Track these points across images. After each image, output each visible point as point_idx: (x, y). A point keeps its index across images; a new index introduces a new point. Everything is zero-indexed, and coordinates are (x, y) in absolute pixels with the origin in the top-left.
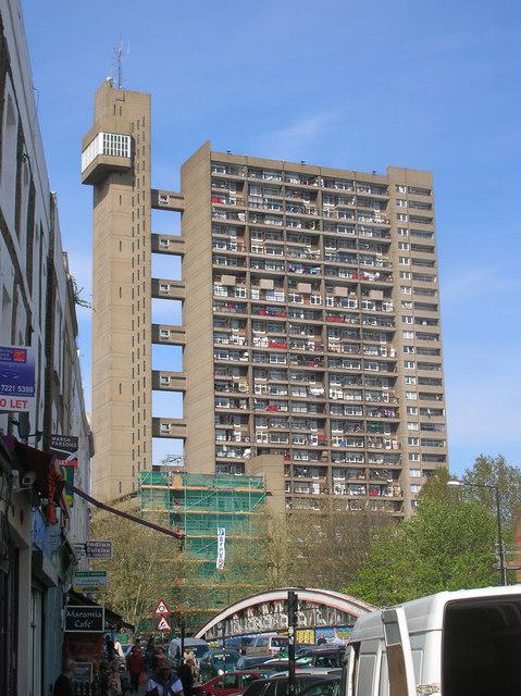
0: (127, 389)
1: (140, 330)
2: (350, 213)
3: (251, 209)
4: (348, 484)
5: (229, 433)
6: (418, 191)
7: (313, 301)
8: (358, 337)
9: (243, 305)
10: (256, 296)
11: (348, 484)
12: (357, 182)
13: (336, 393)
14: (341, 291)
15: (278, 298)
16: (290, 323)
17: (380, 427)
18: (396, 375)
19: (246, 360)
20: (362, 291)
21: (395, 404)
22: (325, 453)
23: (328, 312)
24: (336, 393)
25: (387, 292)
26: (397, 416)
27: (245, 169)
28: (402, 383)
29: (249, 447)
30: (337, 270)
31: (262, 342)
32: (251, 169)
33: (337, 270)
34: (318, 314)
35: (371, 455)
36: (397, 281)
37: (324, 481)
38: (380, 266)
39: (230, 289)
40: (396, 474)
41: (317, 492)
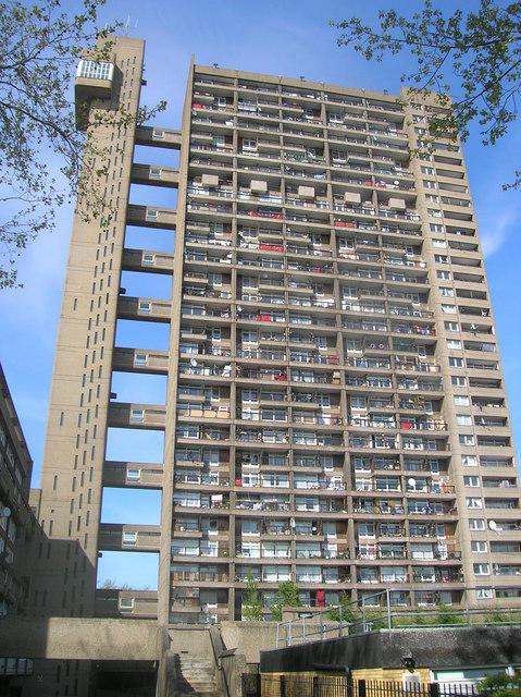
0: (84, 305)
1: (108, 243)
2: (361, 126)
4: (371, 415)
5: (205, 347)
7: (318, 206)
8: (377, 244)
9: (228, 206)
10: (245, 198)
11: (371, 415)
12: (366, 99)
13: (352, 305)
14: (355, 198)
15: (276, 200)
16: (288, 226)
17: (410, 345)
18: (429, 286)
19: (229, 262)
20: (379, 202)
21: (428, 320)
22: (336, 374)
23: (336, 216)
24: (352, 305)
25: (411, 202)
26: (433, 332)
27: (236, 82)
28: (437, 296)
29: (229, 364)
31: (251, 244)
32: (241, 82)
35: (401, 379)
36: (421, 191)
37: (336, 411)
38: (400, 176)
40: (437, 404)
41: (327, 422)
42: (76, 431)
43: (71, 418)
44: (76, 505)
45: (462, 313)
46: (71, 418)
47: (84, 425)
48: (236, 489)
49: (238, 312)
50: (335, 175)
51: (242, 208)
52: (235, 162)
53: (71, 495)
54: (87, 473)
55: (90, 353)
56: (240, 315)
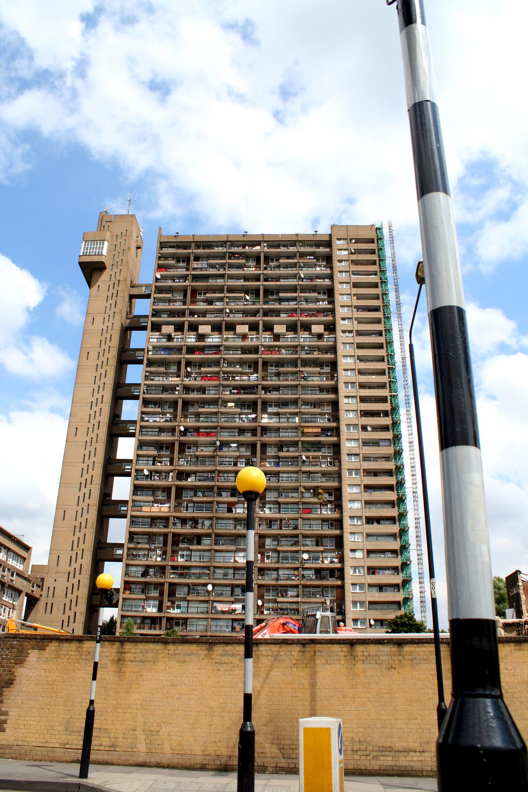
3: (193, 273)
6: (358, 241)
27: (193, 245)
30: (277, 313)
33: (277, 313)
34: (255, 350)
39: (169, 338)
42: (74, 523)
43: (70, 514)
44: (72, 575)
45: (362, 416)
46: (70, 514)
47: (79, 519)
48: (170, 563)
49: (180, 431)
50: (267, 313)
51: (191, 350)
52: (187, 313)
53: (68, 569)
54: (80, 553)
55: (85, 466)
56: (184, 433)
